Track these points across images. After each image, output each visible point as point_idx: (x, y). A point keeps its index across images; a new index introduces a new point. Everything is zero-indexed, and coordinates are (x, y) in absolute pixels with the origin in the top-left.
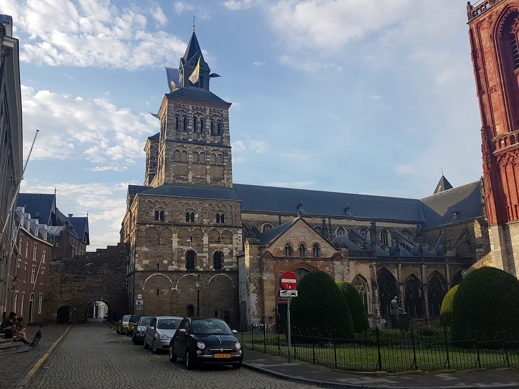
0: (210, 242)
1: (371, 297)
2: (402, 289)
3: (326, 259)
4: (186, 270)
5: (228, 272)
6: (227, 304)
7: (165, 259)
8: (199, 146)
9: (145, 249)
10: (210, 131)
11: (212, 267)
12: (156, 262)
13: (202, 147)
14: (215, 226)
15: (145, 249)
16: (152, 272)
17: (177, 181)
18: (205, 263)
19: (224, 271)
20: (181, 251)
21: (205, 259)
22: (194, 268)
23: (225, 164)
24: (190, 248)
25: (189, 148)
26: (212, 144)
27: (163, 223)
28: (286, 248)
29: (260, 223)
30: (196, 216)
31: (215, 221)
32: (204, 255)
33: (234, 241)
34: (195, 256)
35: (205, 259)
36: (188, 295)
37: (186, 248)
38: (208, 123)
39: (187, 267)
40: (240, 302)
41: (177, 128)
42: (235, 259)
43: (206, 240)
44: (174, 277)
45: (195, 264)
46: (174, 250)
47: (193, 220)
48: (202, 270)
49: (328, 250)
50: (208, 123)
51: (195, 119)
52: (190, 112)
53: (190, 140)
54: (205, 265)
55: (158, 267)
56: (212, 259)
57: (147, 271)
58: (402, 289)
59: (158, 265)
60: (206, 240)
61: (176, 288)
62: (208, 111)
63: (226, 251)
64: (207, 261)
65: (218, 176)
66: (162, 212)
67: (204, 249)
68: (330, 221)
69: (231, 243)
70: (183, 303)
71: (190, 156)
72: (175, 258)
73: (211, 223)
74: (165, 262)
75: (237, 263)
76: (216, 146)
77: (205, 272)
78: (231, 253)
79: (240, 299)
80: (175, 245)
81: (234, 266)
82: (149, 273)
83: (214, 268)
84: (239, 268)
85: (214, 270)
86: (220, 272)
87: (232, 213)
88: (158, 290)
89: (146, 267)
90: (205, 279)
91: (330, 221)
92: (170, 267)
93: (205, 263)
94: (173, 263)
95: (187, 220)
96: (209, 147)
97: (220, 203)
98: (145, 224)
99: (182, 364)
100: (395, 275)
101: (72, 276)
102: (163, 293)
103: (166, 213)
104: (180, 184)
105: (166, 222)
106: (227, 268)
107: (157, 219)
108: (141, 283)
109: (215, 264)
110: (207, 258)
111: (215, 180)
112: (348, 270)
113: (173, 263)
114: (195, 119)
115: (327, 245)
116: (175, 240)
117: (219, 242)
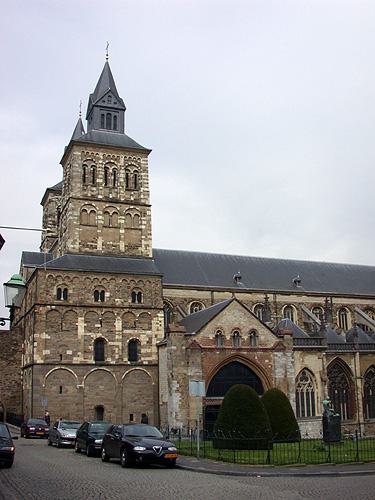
0: (124, 328)
1: (320, 395)
2: (359, 383)
3: (265, 350)
8: (111, 204)
9: (45, 336)
10: (125, 185)
11: (126, 359)
13: (114, 205)
14: (131, 307)
15: (45, 336)
16: (54, 364)
17: (84, 250)
19: (142, 365)
20: (87, 339)
21: (117, 347)
23: (143, 227)
24: (99, 335)
25: (99, 207)
26: (127, 203)
27: (66, 303)
28: (217, 336)
29: (186, 300)
30: (107, 294)
31: (130, 301)
32: (116, 343)
33: (154, 326)
35: (117, 347)
37: (95, 336)
38: (122, 175)
39: (96, 359)
41: (84, 181)
42: (154, 349)
43: (118, 325)
46: (80, 337)
47: (103, 300)
48: (114, 362)
49: (267, 338)
50: (122, 175)
51: (106, 169)
52: (101, 162)
53: (100, 197)
56: (127, 350)
57: (48, 364)
58: (359, 383)
60: (118, 325)
62: (122, 161)
63: (143, 339)
65: (134, 242)
66: (66, 290)
67: (117, 337)
68: (275, 298)
69: (150, 329)
71: (100, 217)
72: (81, 347)
73: (126, 304)
74: (69, 352)
76: (132, 204)
78: (149, 342)
80: (81, 331)
81: (154, 358)
82: (50, 367)
87: (151, 291)
91: (275, 298)
92: (75, 359)
94: (79, 353)
95: (96, 300)
96: (123, 205)
97: (137, 278)
98: (45, 305)
99: (85, 453)
100: (352, 367)
103: (70, 292)
104: (87, 253)
105: (71, 302)
106: (145, 360)
107: (59, 298)
108: (40, 378)
111: (129, 247)
112: (292, 362)
113: (79, 353)
114: (106, 169)
115: (267, 331)
116: (81, 325)
117: (134, 328)
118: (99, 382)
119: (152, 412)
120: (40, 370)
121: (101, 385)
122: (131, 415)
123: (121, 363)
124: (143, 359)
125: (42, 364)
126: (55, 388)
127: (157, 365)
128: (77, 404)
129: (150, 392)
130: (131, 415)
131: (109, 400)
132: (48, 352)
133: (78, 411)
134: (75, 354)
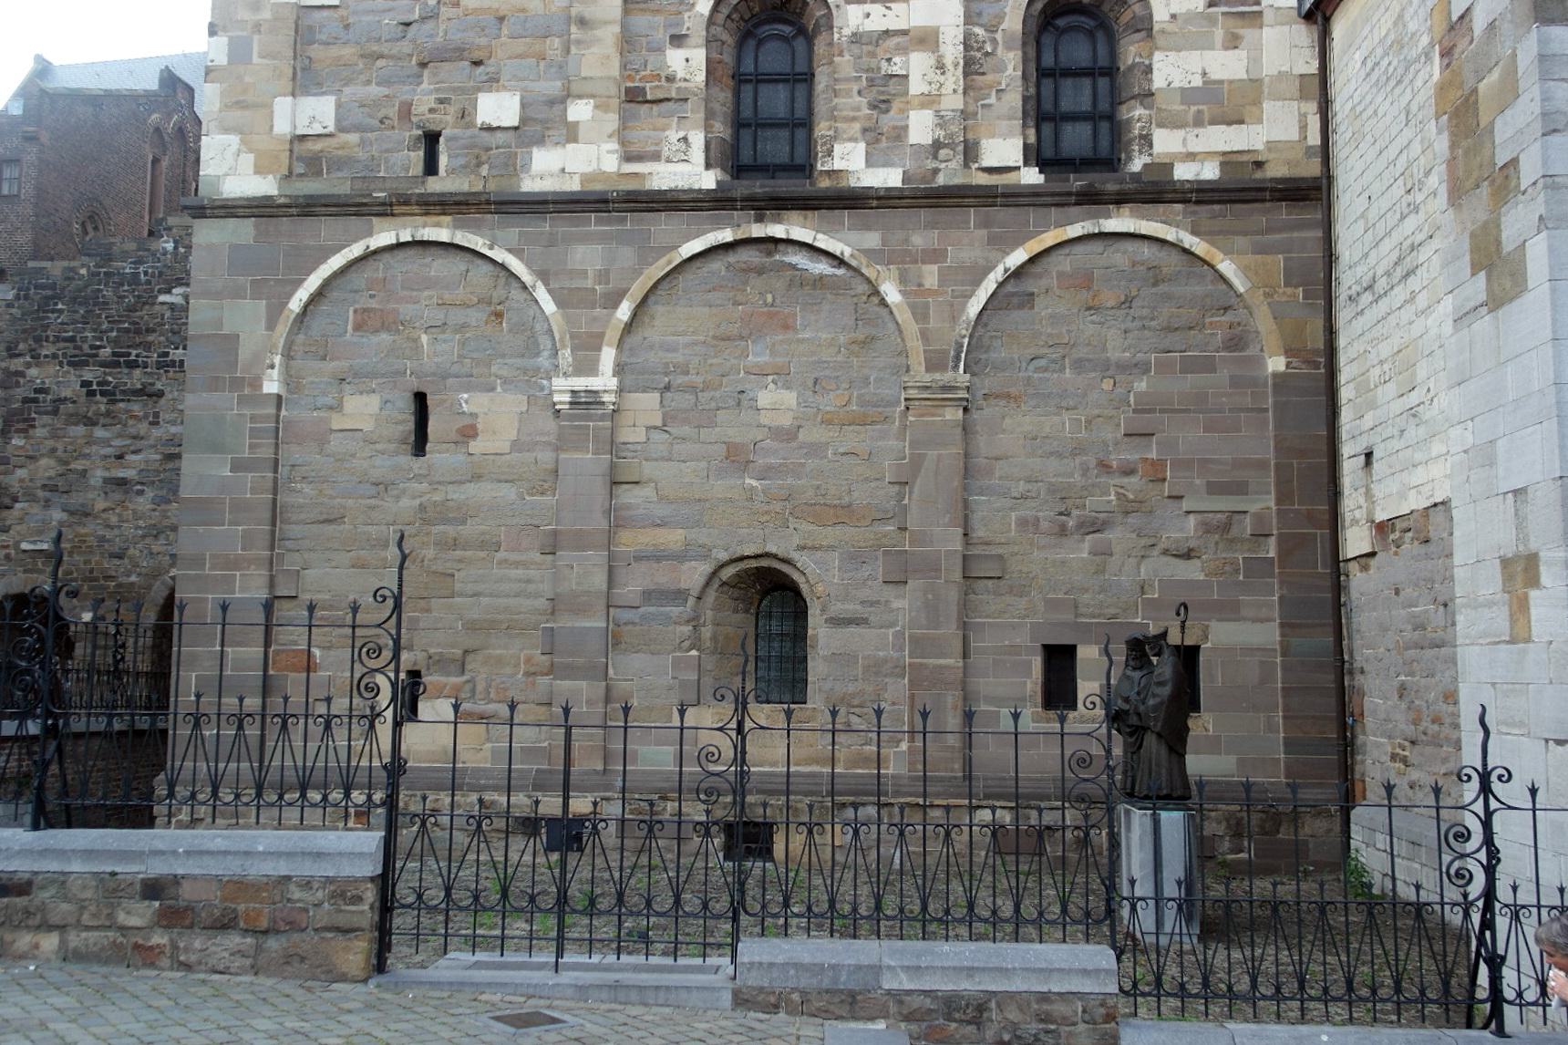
4: (708, 180)
5: (1199, 195)
6: (1192, 571)
7: (493, 82)
11: (1004, 149)
12: (406, 111)
16: (361, 208)
18: (929, 101)
19: (1157, 191)
22: (805, 168)
34: (820, 47)
36: (737, 458)
39: (735, 158)
40: (1356, 541)
44: (589, 252)
45: (822, 129)
48: (889, 178)
54: (921, 128)
55: (431, 167)
56: (1010, 66)
57: (308, 208)
59: (431, 140)
61: (604, 381)
64: (954, 79)
70: (673, 538)
72: (599, 59)
74: (499, 108)
75: (1320, 88)
77: (926, 198)
79: (1352, 502)
81: (1275, 132)
82: (326, 228)
83: (1034, 156)
84: (1340, 140)
85: (1032, 176)
86: (1092, 199)
88: (420, 398)
89: (314, 165)
90: (930, 275)
93: (929, 101)
94: (579, 111)
101: (68, 384)
102: (469, 432)
106: (1190, 151)
108: (245, 321)
109: (1042, 115)
110: (952, 50)
113: (579, 111)
118: (758, 355)
119: (1268, 634)
120: (239, 259)
121: (781, 375)
122: (1059, 660)
123: (950, 173)
124: (1166, 142)
125: (259, 209)
126: (368, 412)
127: (1310, 194)
128: (552, 547)
129: (1260, 443)
130: (1059, 660)
131: (844, 513)
132: (318, 113)
133: (556, 605)
134: (543, 122)
